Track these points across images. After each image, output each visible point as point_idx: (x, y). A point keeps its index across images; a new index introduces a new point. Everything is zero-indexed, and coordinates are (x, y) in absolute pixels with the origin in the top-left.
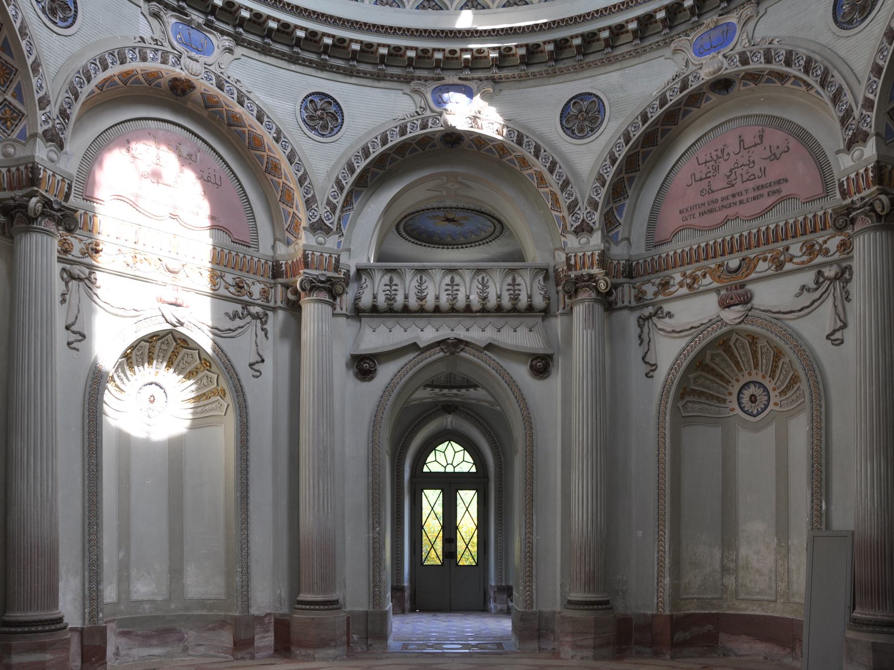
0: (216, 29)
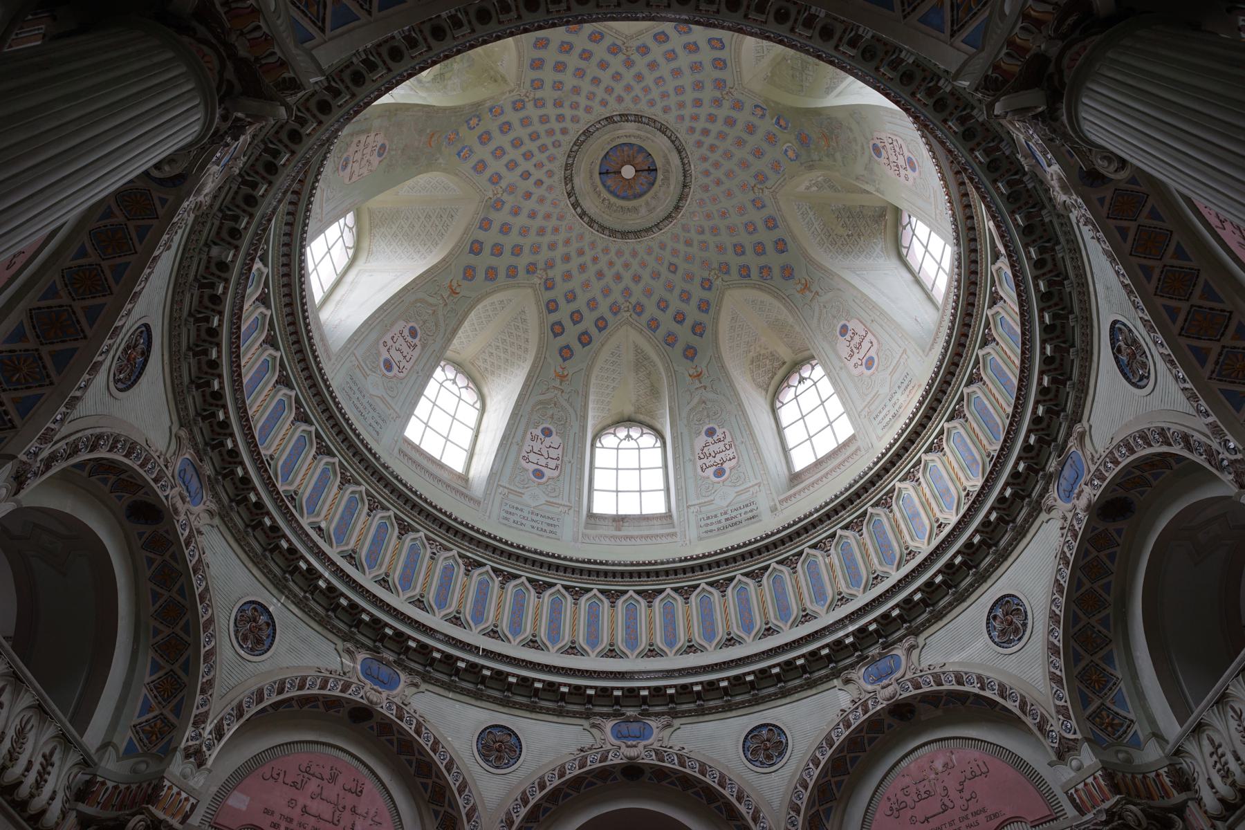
0: (894, 643)
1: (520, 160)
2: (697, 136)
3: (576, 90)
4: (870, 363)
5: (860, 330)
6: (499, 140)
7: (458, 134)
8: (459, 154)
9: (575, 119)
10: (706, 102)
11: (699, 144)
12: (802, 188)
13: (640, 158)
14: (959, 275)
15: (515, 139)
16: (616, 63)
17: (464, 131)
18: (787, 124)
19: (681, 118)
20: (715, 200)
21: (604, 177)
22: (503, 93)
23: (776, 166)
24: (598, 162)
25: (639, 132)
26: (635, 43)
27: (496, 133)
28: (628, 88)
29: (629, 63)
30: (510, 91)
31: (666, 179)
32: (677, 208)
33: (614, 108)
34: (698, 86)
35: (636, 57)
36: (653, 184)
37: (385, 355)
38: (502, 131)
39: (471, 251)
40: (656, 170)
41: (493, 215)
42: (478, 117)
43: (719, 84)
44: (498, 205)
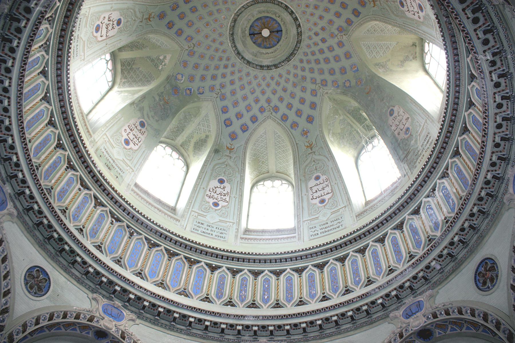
1: (326, 50)
2: (230, 63)
3: (295, 85)
4: (98, 29)
5: (111, 33)
6: (336, 66)
7: (356, 82)
8: (358, 70)
9: (296, 67)
10: (228, 84)
11: (228, 59)
12: (168, 57)
13: (259, 41)
14: (90, 158)
15: (327, 63)
16: (275, 101)
17: (353, 83)
18: (186, 92)
19: (240, 71)
20: (214, 30)
21: (279, 29)
22: (331, 94)
23: (185, 64)
24: (283, 38)
25: (261, 60)
26: (266, 114)
27: (337, 71)
28: (268, 85)
29: (269, 101)
30: (327, 93)
31: (243, 32)
32: (235, 21)
33: (274, 72)
34: (233, 93)
35: (265, 105)
36: (251, 26)
37: (421, 14)
38: (334, 70)
39: (359, 13)
40: (250, 35)
41: (344, 25)
42: (345, 86)
43: (223, 98)
44: (340, 29)
